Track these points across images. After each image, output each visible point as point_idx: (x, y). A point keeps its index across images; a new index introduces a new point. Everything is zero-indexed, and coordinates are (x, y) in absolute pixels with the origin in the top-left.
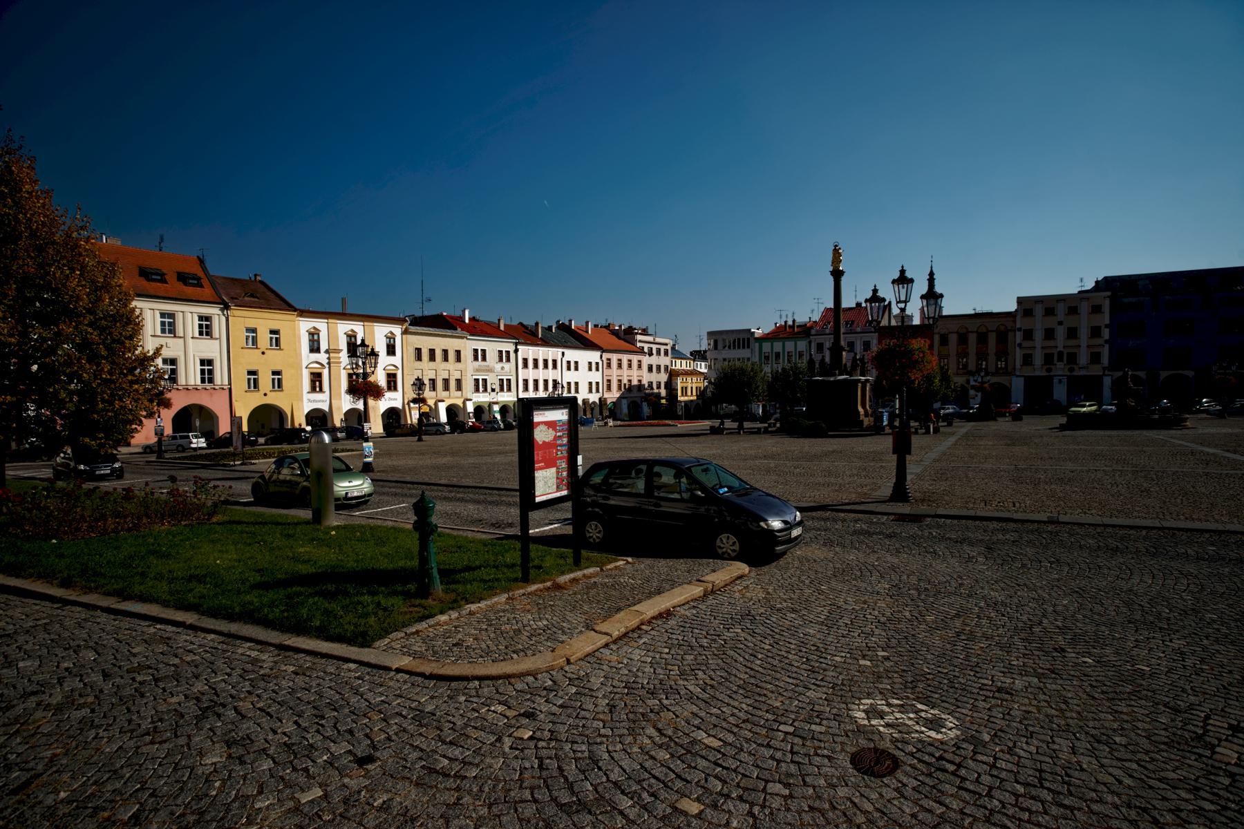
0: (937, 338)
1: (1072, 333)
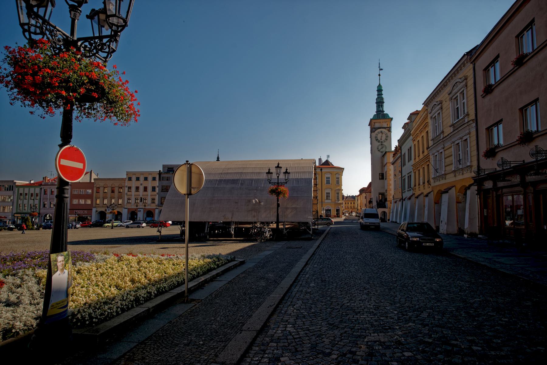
0: (95, 189)
1: (145, 189)
